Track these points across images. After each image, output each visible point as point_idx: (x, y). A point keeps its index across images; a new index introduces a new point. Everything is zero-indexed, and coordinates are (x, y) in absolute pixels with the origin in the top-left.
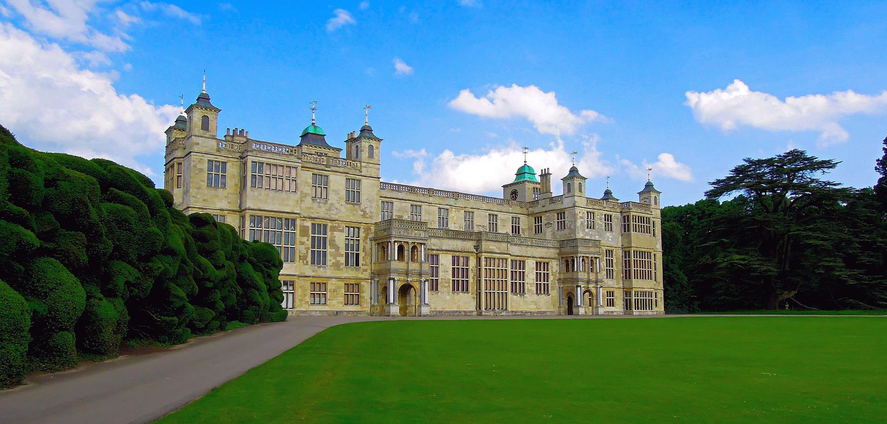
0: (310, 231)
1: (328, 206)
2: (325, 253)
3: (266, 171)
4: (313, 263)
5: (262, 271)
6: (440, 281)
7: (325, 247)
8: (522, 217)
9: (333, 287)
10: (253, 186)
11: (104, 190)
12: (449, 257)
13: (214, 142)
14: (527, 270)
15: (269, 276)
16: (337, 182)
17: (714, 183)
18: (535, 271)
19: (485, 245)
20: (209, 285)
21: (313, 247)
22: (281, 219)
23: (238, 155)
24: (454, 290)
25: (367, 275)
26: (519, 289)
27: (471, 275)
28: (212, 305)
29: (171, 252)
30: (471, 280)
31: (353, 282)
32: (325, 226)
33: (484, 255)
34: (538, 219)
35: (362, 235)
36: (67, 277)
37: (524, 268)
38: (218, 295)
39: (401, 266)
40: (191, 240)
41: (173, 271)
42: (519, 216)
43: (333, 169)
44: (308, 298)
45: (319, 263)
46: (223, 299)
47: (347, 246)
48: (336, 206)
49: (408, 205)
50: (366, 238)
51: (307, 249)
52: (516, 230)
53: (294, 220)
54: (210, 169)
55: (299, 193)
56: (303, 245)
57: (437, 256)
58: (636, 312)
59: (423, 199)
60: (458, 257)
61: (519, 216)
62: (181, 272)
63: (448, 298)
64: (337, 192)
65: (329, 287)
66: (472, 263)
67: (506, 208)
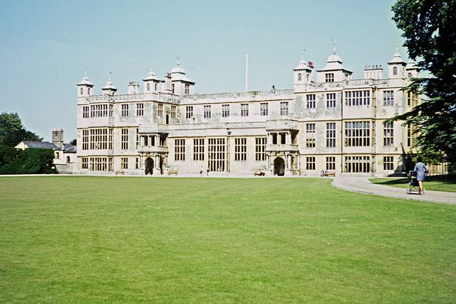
12: (192, 140)
26: (241, 156)
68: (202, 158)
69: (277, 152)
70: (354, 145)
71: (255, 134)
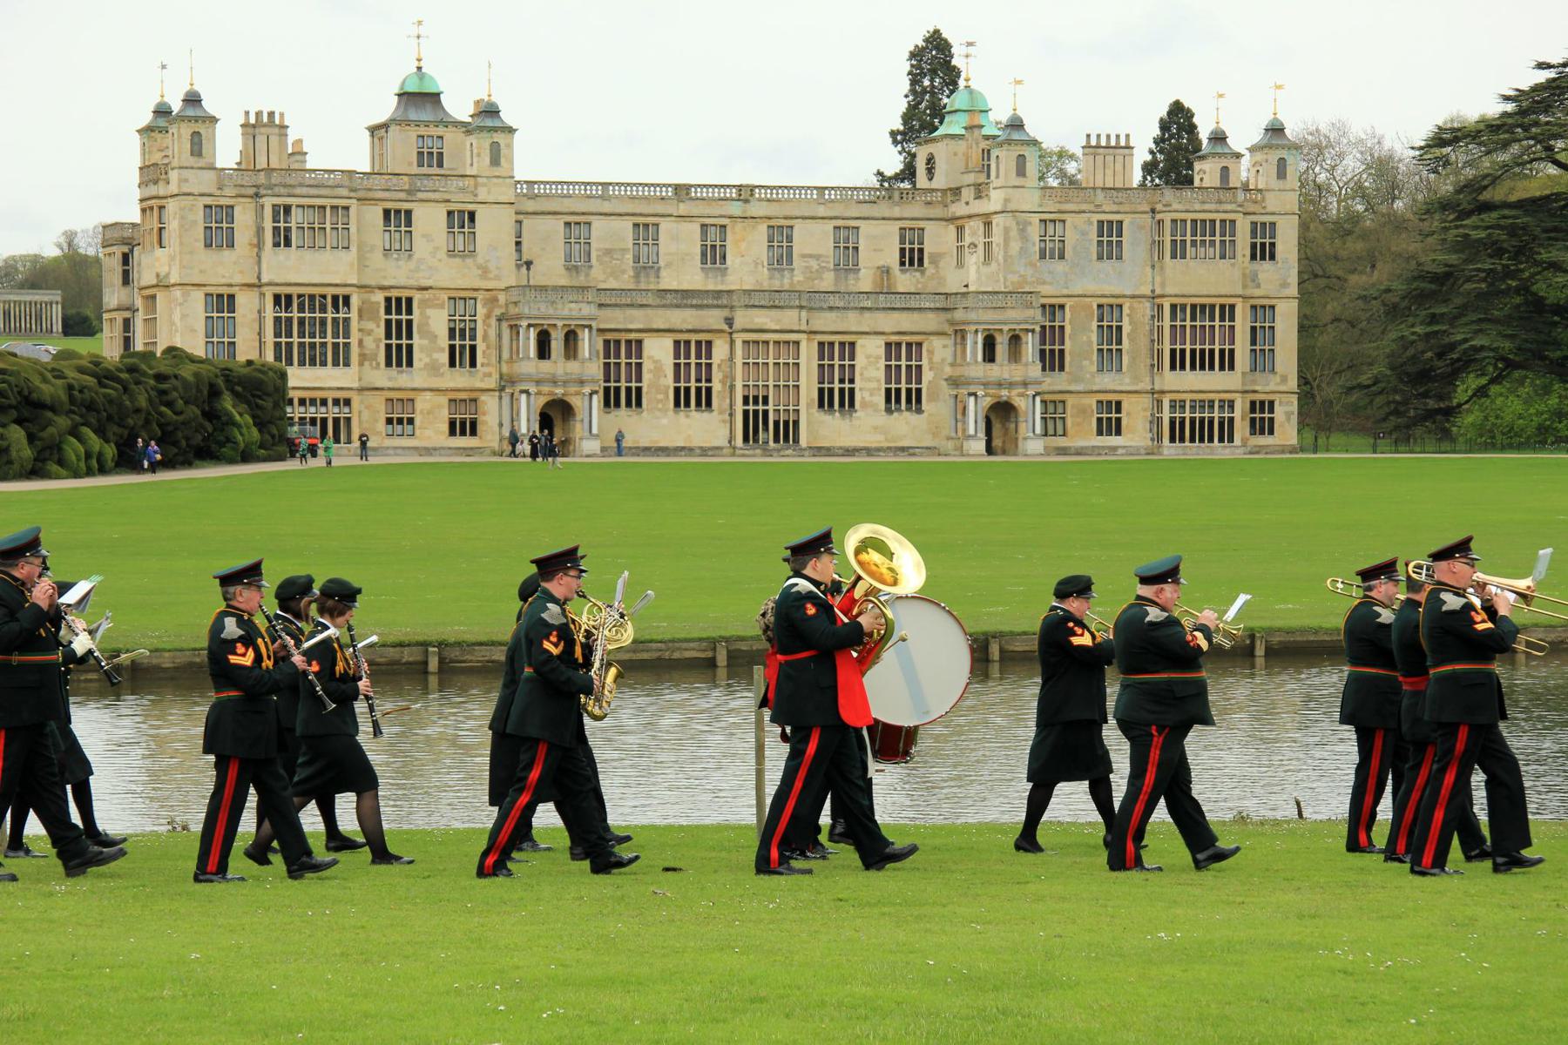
0: (382, 310)
1: (412, 265)
2: (410, 348)
3: (297, 217)
4: (389, 364)
5: (248, 403)
6: (644, 390)
7: (410, 336)
9: (427, 406)
10: (277, 245)
11: (100, 383)
12: (667, 343)
13: (211, 175)
14: (860, 361)
15: (257, 406)
16: (429, 220)
17: (1507, 98)
18: (882, 363)
19: (742, 318)
20: (170, 428)
21: (388, 336)
22: (324, 297)
23: (251, 191)
24: (677, 404)
25: (492, 383)
26: (837, 397)
27: (717, 376)
28: (175, 443)
29: (138, 411)
30: (716, 386)
31: (463, 396)
32: (409, 301)
33: (739, 339)
34: (960, 229)
35: (481, 311)
36: (92, 435)
37: (852, 358)
38: (180, 434)
39: (545, 366)
40: (153, 393)
41: (140, 423)
42: (921, 224)
43: (420, 195)
44: (381, 425)
45: (399, 364)
46: (188, 439)
47: (452, 332)
48: (429, 261)
49: (626, 225)
50: (488, 316)
51: (378, 341)
52: (912, 257)
53: (347, 300)
54: (208, 217)
55: (354, 249)
56: (368, 334)
57: (639, 342)
58: (1169, 450)
59: (660, 209)
60: (688, 343)
61: (921, 224)
62: (147, 422)
63: (665, 421)
64: (427, 237)
65: (419, 405)
66: (720, 351)
67: (883, 209)
68: (705, 400)
69: (1000, 385)
70: (1193, 367)
71: (887, 330)
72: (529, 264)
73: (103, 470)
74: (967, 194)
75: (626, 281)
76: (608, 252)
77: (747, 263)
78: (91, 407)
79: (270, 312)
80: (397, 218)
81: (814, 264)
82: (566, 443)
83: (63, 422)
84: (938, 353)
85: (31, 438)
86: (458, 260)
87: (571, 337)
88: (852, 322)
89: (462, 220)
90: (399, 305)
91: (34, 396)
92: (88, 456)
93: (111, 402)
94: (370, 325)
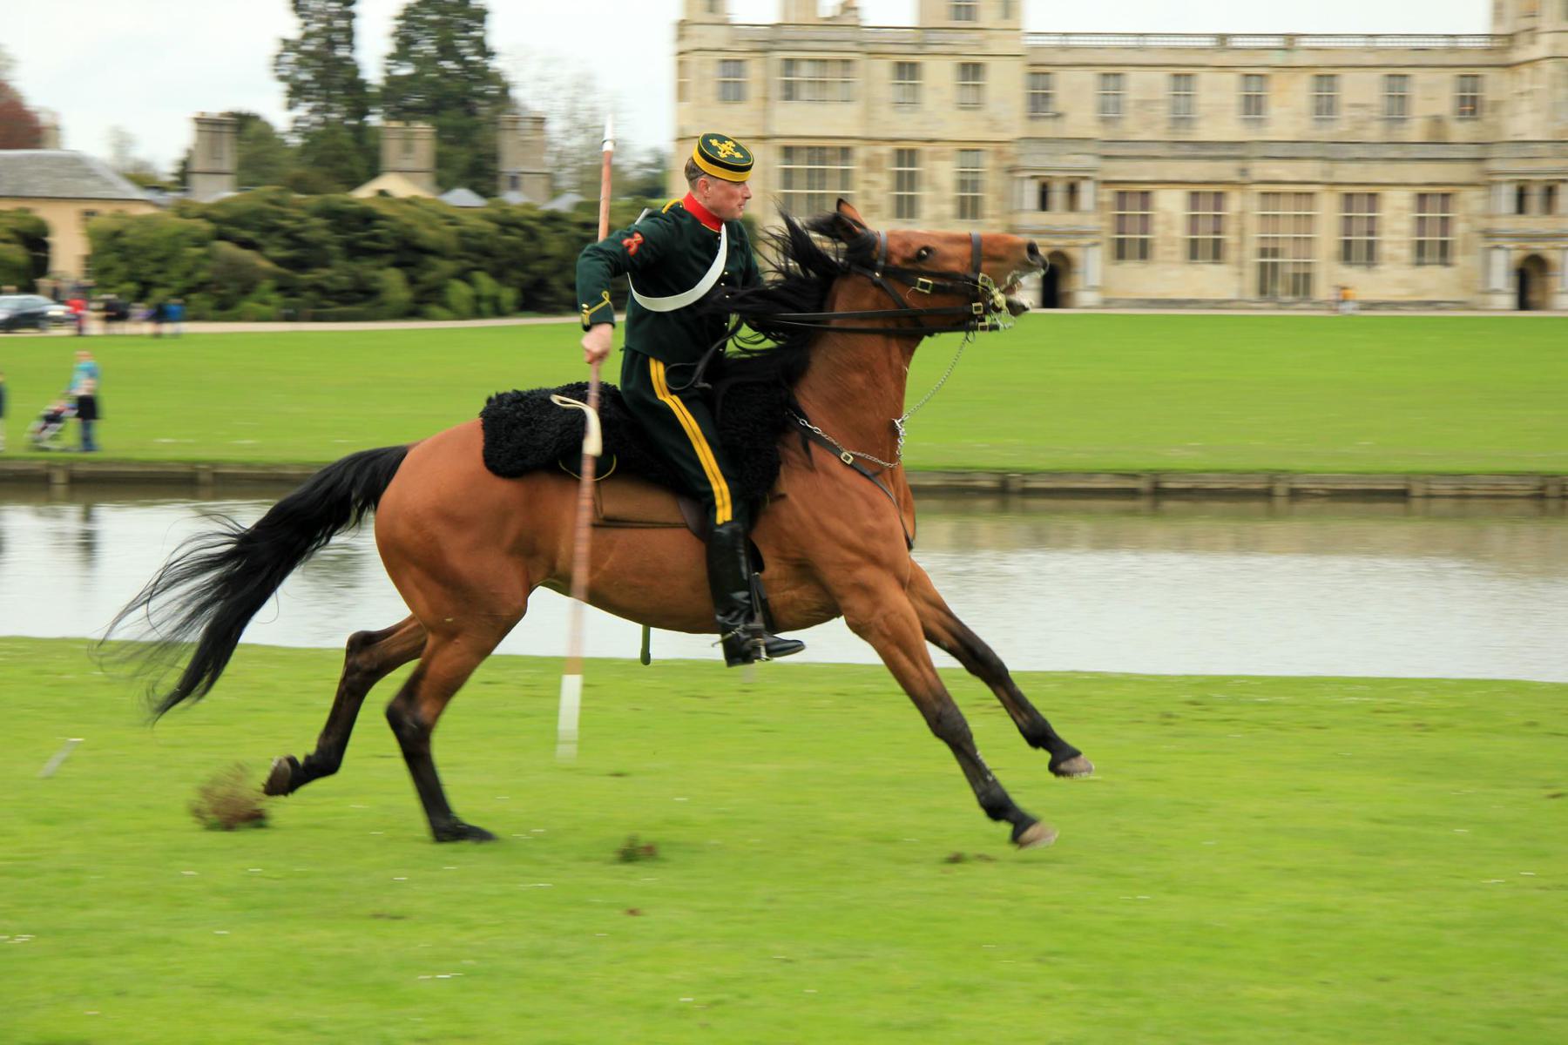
3: (805, 72)
8: (1491, 76)
13: (722, 30)
16: (939, 74)
30: (1230, 238)
39: (1044, 219)
48: (938, 110)
49: (1160, 78)
52: (1470, 106)
66: (1234, 203)
68: (1217, 252)
72: (1058, 116)
73: (499, 312)
74: (1524, 38)
75: (1159, 132)
76: (1143, 103)
77: (1288, 114)
78: (486, 252)
79: (778, 164)
80: (907, 71)
81: (1359, 113)
82: (1068, 295)
83: (448, 266)
84: (1470, 203)
85: (412, 281)
86: (963, 113)
87: (1072, 190)
88: (1378, 173)
89: (971, 71)
90: (906, 156)
91: (419, 242)
92: (478, 298)
93: (514, 248)
94: (874, 177)
